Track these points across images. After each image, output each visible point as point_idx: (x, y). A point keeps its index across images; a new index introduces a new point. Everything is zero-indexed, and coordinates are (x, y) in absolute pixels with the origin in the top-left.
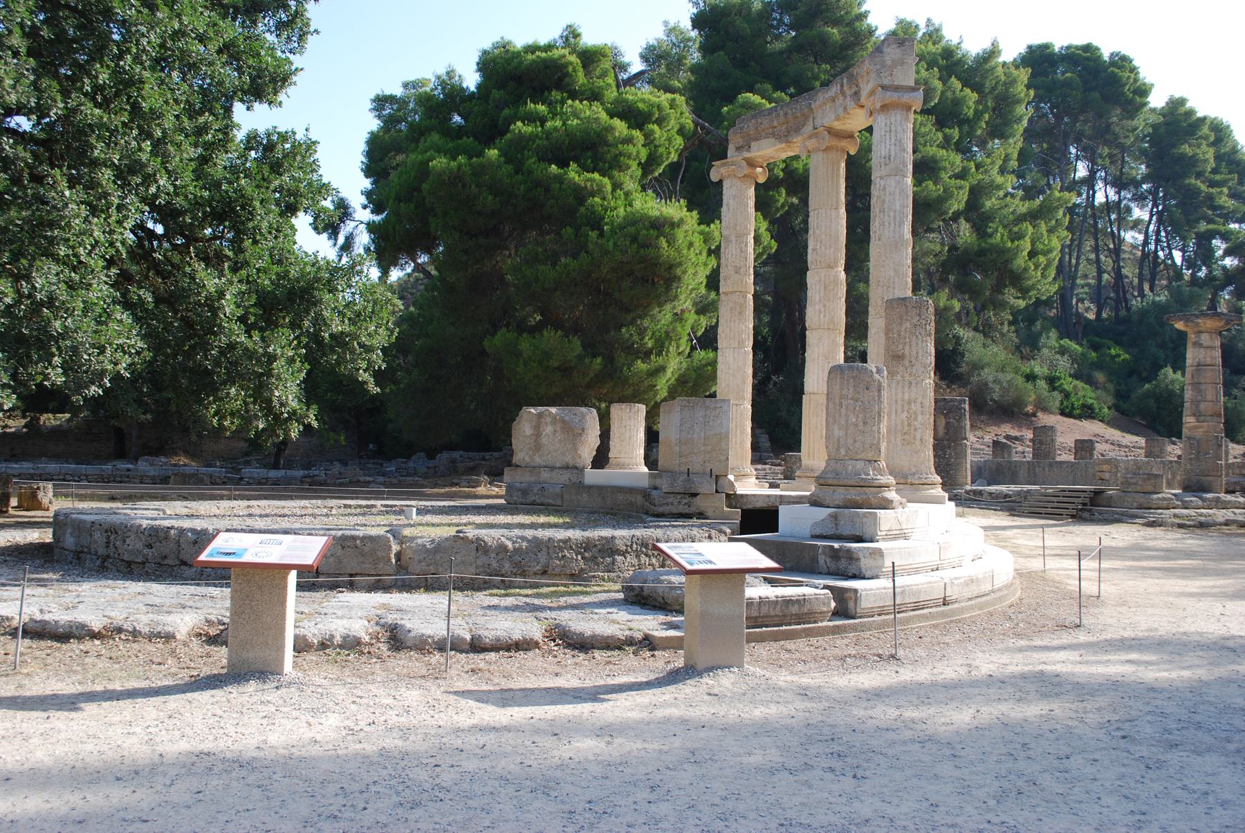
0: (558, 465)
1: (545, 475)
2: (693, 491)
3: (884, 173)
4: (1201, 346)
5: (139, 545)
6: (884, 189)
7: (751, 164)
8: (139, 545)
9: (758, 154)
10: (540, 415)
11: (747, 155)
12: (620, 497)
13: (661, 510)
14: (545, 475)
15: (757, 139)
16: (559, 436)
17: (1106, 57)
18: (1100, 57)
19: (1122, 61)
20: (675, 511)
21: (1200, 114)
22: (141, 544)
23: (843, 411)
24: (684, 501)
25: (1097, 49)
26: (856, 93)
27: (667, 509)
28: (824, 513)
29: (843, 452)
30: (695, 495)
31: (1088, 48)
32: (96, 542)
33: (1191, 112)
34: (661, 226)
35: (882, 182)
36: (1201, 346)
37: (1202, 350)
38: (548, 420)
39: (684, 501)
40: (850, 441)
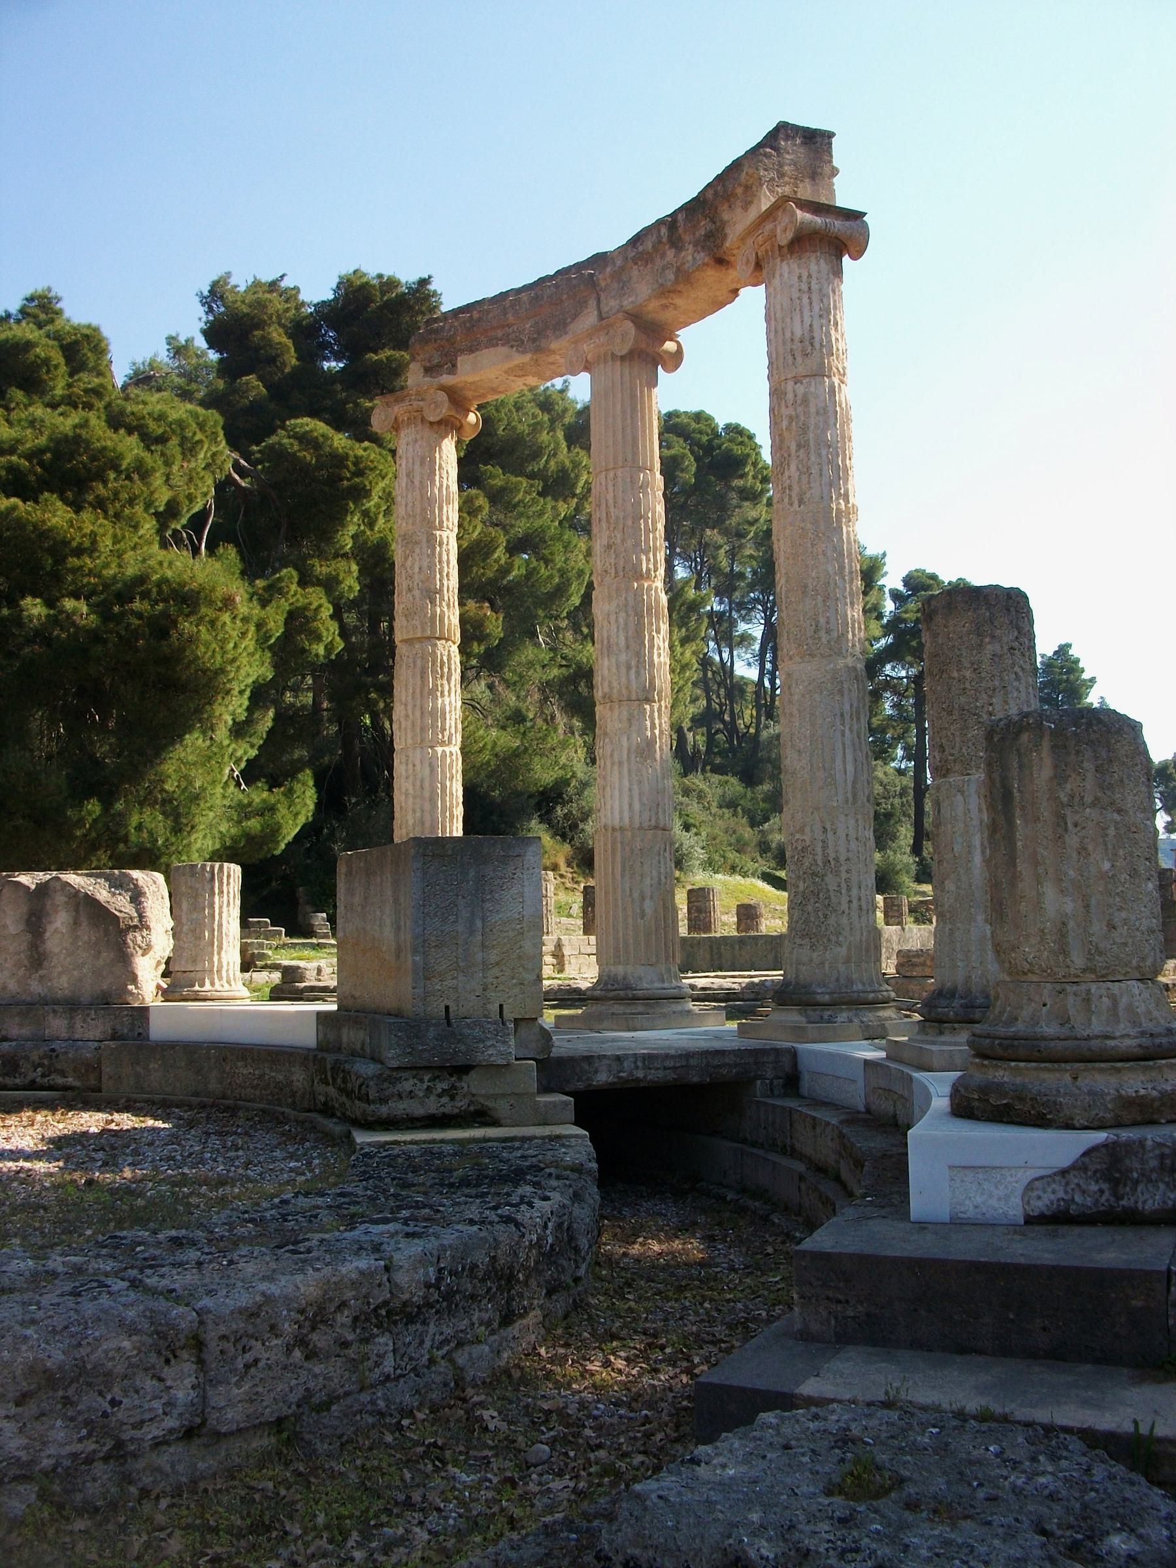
0: (85, 998)
1: (57, 1025)
2: (461, 1060)
3: (801, 371)
6: (805, 401)
7: (458, 400)
9: (470, 379)
10: (43, 888)
11: (446, 379)
12: (244, 1070)
13: (384, 1110)
14: (57, 1025)
15: (471, 350)
20: (420, 1111)
23: (1072, 840)
24: (441, 1086)
26: (710, 235)
27: (400, 1108)
28: (1060, 1147)
30: (463, 1070)
34: (187, 599)
35: (801, 389)
39: (441, 1086)
40: (1098, 928)
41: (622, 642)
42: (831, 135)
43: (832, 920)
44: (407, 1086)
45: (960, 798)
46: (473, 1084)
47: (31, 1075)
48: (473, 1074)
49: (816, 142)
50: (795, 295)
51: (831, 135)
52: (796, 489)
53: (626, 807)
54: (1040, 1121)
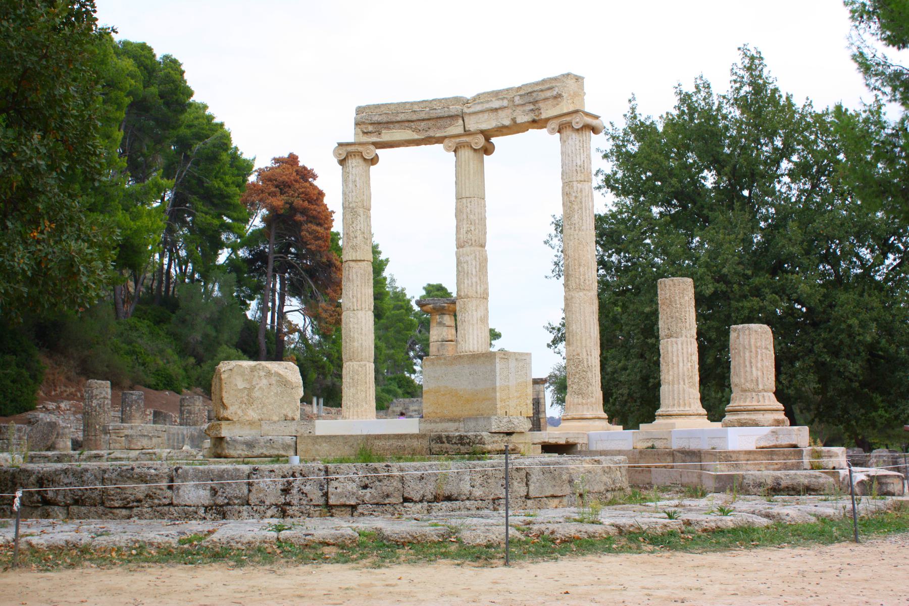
4: (444, 325)
5: (352, 487)
6: (581, 191)
8: (352, 487)
10: (253, 369)
13: (489, 447)
16: (274, 389)
17: (159, 57)
18: (154, 56)
19: (173, 64)
21: (217, 120)
22: (354, 485)
25: (150, 49)
29: (761, 387)
31: (143, 46)
32: (260, 491)
33: (210, 118)
36: (444, 325)
37: (445, 328)
38: (262, 374)
40: (765, 379)
41: (474, 273)
42: (583, 78)
43: (590, 388)
44: (496, 439)
45: (675, 345)
46: (514, 438)
47: (261, 451)
48: (514, 435)
49: (578, 79)
50: (578, 148)
51: (583, 78)
52: (577, 226)
53: (475, 342)
54: (757, 425)
